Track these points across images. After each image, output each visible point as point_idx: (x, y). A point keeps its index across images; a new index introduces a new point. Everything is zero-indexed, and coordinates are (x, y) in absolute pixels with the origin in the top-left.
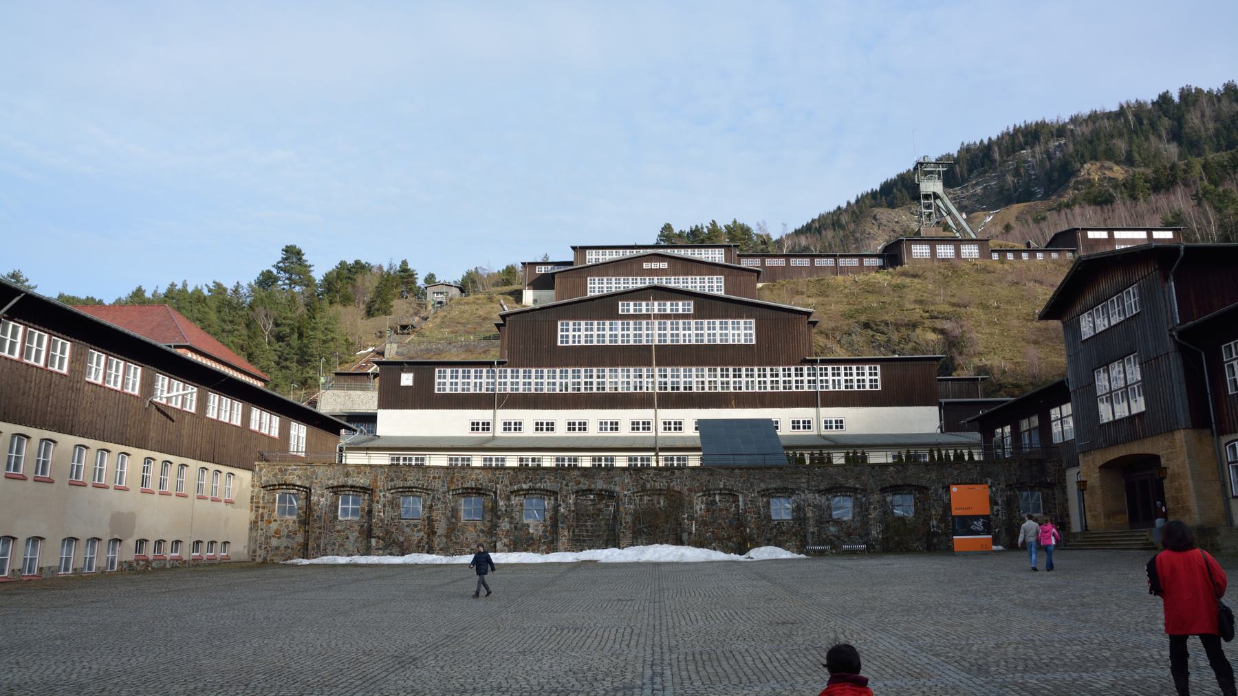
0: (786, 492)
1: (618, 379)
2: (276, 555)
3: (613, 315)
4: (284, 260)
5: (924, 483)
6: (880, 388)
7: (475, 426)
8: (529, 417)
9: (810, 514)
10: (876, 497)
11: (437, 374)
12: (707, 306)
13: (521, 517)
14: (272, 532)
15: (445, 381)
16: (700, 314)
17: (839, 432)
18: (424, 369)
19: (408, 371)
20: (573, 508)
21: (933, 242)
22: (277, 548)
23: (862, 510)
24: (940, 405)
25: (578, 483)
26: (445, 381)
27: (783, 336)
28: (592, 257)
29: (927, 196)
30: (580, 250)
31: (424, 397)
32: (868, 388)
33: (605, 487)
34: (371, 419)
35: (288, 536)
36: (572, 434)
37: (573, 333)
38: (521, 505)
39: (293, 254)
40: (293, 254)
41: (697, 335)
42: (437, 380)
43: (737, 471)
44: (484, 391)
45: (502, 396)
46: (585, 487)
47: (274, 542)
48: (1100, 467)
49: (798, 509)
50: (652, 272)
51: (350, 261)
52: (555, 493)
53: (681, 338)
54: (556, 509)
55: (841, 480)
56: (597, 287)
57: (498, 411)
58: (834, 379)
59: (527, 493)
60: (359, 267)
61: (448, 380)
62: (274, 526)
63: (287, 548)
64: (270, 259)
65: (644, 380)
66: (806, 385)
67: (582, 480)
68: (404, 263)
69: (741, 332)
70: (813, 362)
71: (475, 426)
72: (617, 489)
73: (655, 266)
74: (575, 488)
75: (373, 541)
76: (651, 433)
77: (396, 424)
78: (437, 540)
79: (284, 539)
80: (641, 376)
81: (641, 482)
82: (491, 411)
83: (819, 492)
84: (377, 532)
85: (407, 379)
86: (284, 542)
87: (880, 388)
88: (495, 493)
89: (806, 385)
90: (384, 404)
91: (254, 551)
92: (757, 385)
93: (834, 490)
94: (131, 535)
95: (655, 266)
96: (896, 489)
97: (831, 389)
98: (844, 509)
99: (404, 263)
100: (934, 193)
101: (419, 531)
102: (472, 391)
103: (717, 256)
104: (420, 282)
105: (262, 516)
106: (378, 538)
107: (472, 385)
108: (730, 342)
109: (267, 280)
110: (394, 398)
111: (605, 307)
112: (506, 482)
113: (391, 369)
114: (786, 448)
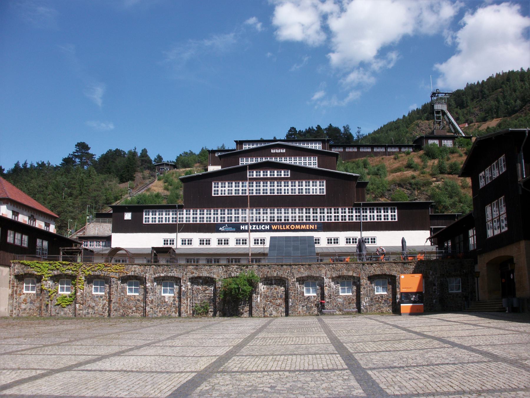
1: (247, 215)
2: (24, 313)
3: (244, 178)
4: (77, 151)
6: (396, 220)
8: (196, 237)
12: (300, 173)
13: (161, 292)
14: (22, 300)
16: (293, 178)
17: (373, 245)
19: (128, 211)
21: (441, 138)
22: (25, 309)
24: (431, 230)
25: (193, 273)
26: (149, 218)
27: (345, 191)
28: (246, 147)
29: (438, 112)
30: (240, 143)
31: (137, 226)
32: (390, 220)
33: (208, 275)
34: (108, 239)
35: (31, 303)
36: (202, 246)
37: (222, 189)
39: (83, 147)
40: (83, 147)
41: (292, 189)
43: (285, 267)
44: (171, 222)
46: (196, 276)
47: (23, 306)
48: (487, 264)
50: (276, 155)
53: (283, 191)
56: (244, 162)
57: (179, 234)
58: (371, 216)
60: (118, 153)
62: (23, 297)
63: (30, 309)
64: (69, 150)
65: (262, 215)
66: (354, 218)
67: (195, 271)
68: (144, 151)
69: (317, 188)
71: (166, 242)
72: (215, 276)
73: (278, 151)
74: (191, 276)
75: (77, 305)
76: (247, 246)
77: (122, 241)
78: (112, 305)
79: (28, 304)
80: (259, 213)
81: (229, 272)
87: (396, 220)
88: (145, 278)
89: (354, 218)
90: (115, 230)
91: (12, 311)
92: (326, 218)
95: (278, 151)
97: (369, 220)
100: (442, 110)
101: (103, 300)
102: (164, 222)
103: (318, 146)
105: (16, 292)
106: (80, 303)
108: (311, 193)
109: (68, 161)
110: (121, 227)
112: (152, 272)
114: (318, 254)
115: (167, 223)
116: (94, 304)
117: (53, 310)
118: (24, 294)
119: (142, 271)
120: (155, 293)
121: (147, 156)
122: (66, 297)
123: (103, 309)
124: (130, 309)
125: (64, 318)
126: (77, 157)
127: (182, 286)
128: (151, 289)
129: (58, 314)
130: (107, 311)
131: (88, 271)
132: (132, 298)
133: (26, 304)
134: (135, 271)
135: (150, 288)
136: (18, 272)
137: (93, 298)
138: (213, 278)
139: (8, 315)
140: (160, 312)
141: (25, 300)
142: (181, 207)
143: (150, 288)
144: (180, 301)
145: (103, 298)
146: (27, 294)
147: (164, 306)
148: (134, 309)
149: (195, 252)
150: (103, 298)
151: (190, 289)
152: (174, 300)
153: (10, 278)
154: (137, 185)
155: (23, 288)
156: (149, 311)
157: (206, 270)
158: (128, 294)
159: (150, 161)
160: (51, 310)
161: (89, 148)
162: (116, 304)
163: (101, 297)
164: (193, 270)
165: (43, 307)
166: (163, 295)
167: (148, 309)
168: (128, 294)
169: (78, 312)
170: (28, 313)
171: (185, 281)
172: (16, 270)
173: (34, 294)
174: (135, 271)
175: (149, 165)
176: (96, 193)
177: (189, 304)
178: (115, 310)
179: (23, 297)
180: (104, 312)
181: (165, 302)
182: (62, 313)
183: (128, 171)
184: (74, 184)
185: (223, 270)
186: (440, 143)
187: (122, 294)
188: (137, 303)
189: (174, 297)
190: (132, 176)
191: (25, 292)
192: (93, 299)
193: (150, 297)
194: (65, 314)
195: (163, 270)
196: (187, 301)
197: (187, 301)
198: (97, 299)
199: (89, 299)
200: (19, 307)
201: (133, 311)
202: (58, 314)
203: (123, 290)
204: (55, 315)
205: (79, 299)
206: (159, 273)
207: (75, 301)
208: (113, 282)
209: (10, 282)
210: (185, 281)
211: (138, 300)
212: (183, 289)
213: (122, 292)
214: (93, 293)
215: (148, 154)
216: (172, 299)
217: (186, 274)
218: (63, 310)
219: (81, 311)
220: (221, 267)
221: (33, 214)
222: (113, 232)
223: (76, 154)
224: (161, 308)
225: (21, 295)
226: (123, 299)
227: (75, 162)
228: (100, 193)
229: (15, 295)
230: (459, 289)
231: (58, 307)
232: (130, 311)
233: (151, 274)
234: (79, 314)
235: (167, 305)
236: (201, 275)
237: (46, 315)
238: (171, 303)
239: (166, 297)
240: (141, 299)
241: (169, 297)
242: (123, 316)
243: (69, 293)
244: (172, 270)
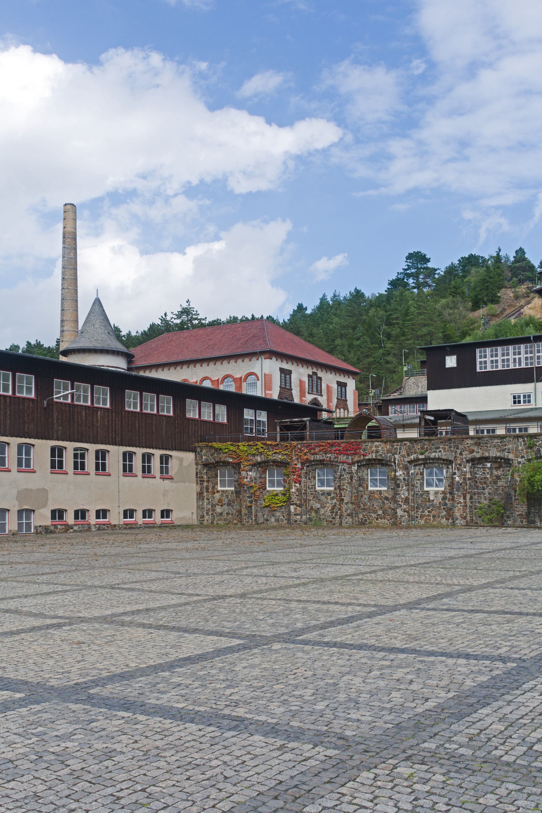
2: (221, 520)
7: (516, 400)
11: (478, 354)
13: (422, 485)
18: (466, 353)
19: (451, 354)
20: (468, 476)
22: (221, 514)
25: (472, 451)
26: (487, 360)
31: (468, 376)
33: (498, 454)
34: (424, 400)
35: (229, 504)
38: (422, 474)
39: (418, 259)
42: (478, 360)
44: (523, 366)
46: (478, 456)
47: (219, 509)
61: (488, 359)
63: (228, 514)
64: (400, 265)
67: (476, 449)
68: (521, 252)
72: (511, 456)
74: (470, 456)
75: (292, 508)
79: (225, 507)
82: (533, 384)
85: (451, 362)
90: (431, 387)
91: (203, 517)
94: (44, 505)
99: (521, 252)
101: (332, 499)
102: (512, 367)
105: (207, 489)
106: (296, 504)
107: (511, 361)
110: (441, 380)
112: (404, 452)
115: (517, 367)
116: (318, 506)
117: (260, 514)
118: (218, 492)
119: (388, 451)
120: (413, 486)
121: (525, 259)
122: (277, 495)
123: (332, 512)
124: (375, 512)
125: (274, 528)
126: (409, 276)
127: (455, 474)
128: (404, 479)
129: (267, 520)
130: (338, 517)
131: (305, 454)
132: (376, 496)
133: (222, 506)
134: (377, 452)
135: (402, 478)
136: (207, 459)
137: (316, 496)
138: (509, 460)
139: (196, 522)
140: (422, 517)
141: (220, 501)
143: (402, 478)
144: (453, 499)
145: (332, 495)
146: (223, 491)
147: (428, 508)
148: (380, 512)
149: (502, 415)
150: (332, 495)
151: (469, 479)
152: (444, 498)
153: (197, 469)
154: (504, 310)
155: (217, 484)
156: (402, 516)
157: (495, 446)
158: (370, 489)
159: (531, 268)
160: (256, 516)
161: (428, 260)
162: (350, 505)
163: (329, 494)
164: (472, 447)
165: (244, 511)
166: (426, 489)
167: (400, 512)
168: (370, 489)
169: (293, 518)
170: (225, 520)
171: (460, 465)
172: (204, 457)
173: (232, 492)
174: (377, 452)
175: (529, 274)
176: (425, 330)
177: (468, 504)
178: (348, 515)
179: (217, 496)
180: (333, 518)
181: (429, 500)
182: (273, 520)
183: (487, 288)
184: (397, 319)
185: (525, 444)
187: (361, 489)
188: (384, 503)
189: (443, 492)
190: (495, 295)
191: (220, 488)
192: (317, 497)
193: (403, 493)
194: (277, 520)
195: (422, 448)
196: (465, 498)
197: (465, 498)
198: (323, 498)
199: (311, 498)
200: (214, 510)
201: (378, 515)
202: (267, 520)
203: (362, 481)
204: (263, 523)
205: (294, 499)
206: (415, 453)
207: (289, 501)
208: (344, 470)
209: (197, 474)
210: (460, 465)
211: (386, 498)
212: (457, 479)
213: (360, 485)
214: (317, 488)
215: (526, 256)
216: (440, 496)
217: (461, 454)
218: (273, 515)
219: (299, 517)
220: (521, 440)
221: (315, 370)
222: (429, 389)
223: (408, 272)
224: (423, 512)
225: (214, 493)
226: (362, 496)
227: (408, 284)
228: (431, 329)
229: (205, 494)
231: (266, 510)
232: (374, 515)
233: (404, 456)
234: (296, 521)
235: (433, 505)
236: (487, 454)
237: (248, 522)
238: (440, 503)
239: (432, 493)
240: (390, 497)
241: (436, 493)
242: (362, 523)
243: (282, 489)
244: (437, 448)
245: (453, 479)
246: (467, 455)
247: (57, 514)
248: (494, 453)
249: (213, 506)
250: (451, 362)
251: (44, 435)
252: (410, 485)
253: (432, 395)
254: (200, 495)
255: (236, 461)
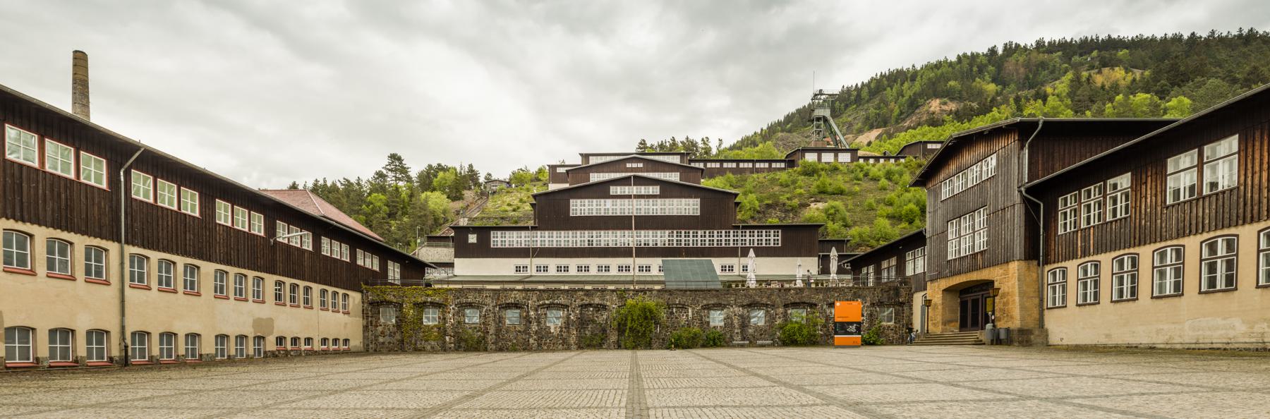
0: (719, 306)
5: (814, 301)
7: (518, 269)
8: (552, 263)
9: (736, 321)
10: (781, 310)
12: (669, 190)
14: (379, 333)
15: (498, 240)
18: (484, 232)
23: (771, 319)
26: (498, 240)
28: (593, 161)
30: (586, 157)
31: (484, 250)
37: (580, 207)
45: (535, 250)
47: (381, 340)
49: (728, 318)
51: (434, 165)
52: (567, 306)
54: (568, 318)
55: (758, 299)
56: (595, 178)
59: (549, 307)
60: (441, 168)
62: (380, 329)
64: (381, 163)
68: (471, 166)
69: (689, 206)
70: (738, 227)
73: (635, 165)
75: (447, 338)
76: (632, 273)
83: (743, 306)
84: (449, 331)
86: (388, 339)
93: (753, 305)
95: (635, 165)
96: (795, 305)
98: (758, 318)
99: (471, 166)
103: (676, 160)
104: (482, 180)
110: (464, 250)
111: (601, 191)
113: (462, 231)
142: (534, 228)
167: (531, 341)
179: (380, 329)
186: (819, 159)
193: (534, 327)
230: (890, 320)
245: (568, 318)
246: (578, 302)
247: (280, 340)
248: (597, 301)
249: (376, 337)
250: (472, 239)
251: (272, 271)
252: (539, 323)
253: (458, 262)
254: (366, 328)
255: (400, 300)
